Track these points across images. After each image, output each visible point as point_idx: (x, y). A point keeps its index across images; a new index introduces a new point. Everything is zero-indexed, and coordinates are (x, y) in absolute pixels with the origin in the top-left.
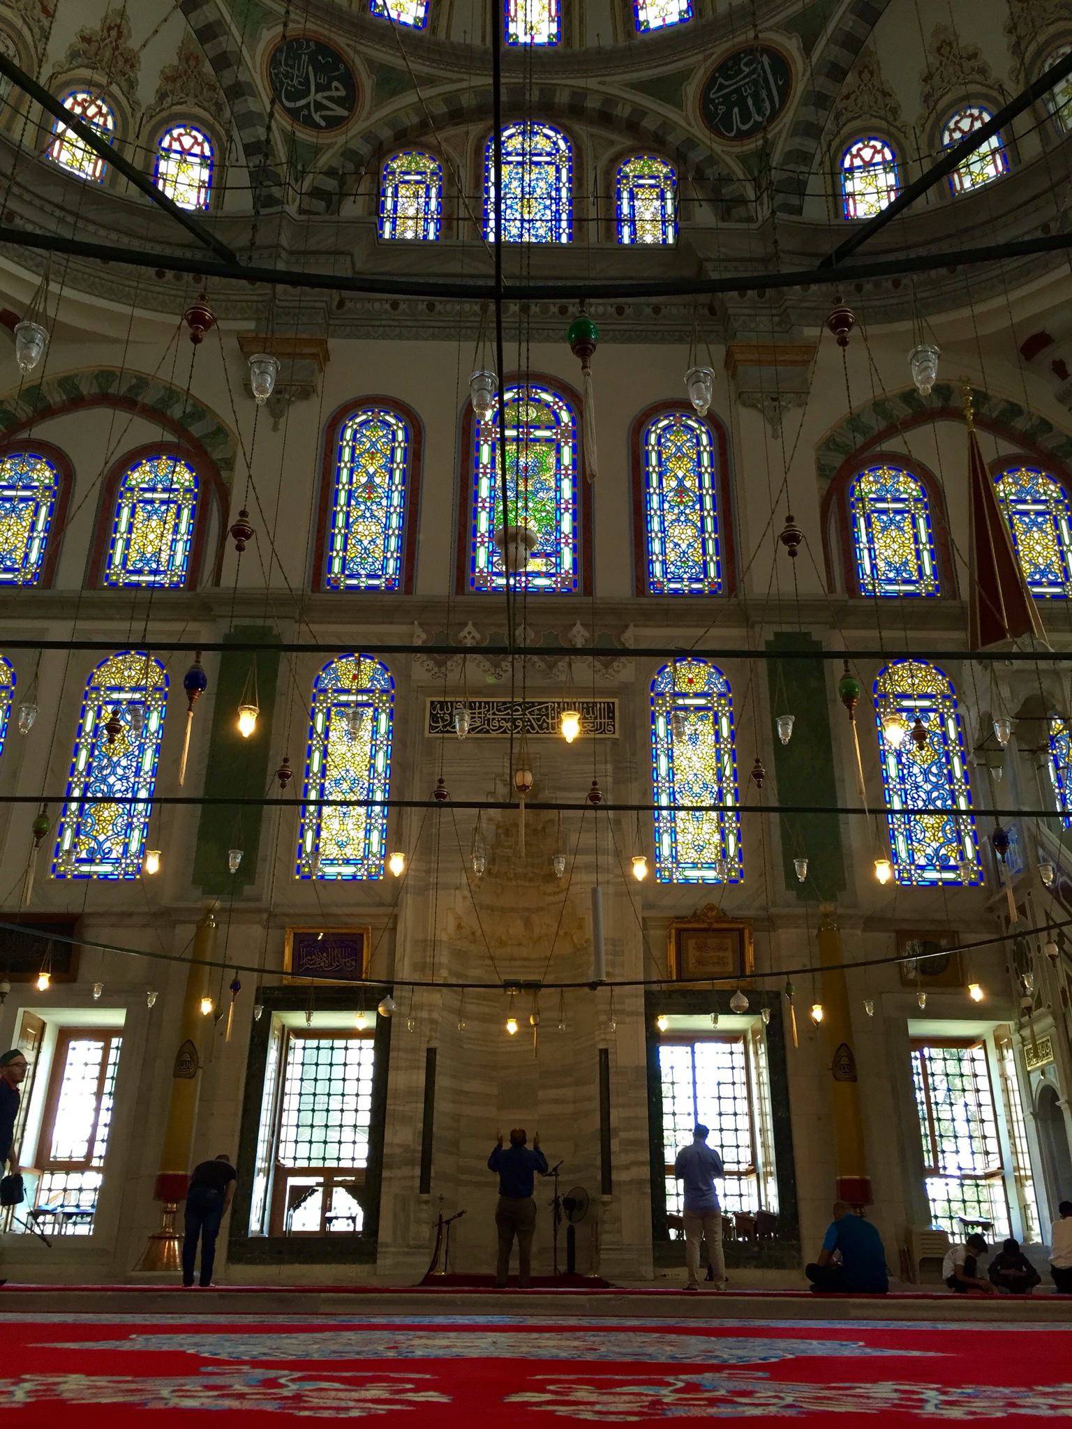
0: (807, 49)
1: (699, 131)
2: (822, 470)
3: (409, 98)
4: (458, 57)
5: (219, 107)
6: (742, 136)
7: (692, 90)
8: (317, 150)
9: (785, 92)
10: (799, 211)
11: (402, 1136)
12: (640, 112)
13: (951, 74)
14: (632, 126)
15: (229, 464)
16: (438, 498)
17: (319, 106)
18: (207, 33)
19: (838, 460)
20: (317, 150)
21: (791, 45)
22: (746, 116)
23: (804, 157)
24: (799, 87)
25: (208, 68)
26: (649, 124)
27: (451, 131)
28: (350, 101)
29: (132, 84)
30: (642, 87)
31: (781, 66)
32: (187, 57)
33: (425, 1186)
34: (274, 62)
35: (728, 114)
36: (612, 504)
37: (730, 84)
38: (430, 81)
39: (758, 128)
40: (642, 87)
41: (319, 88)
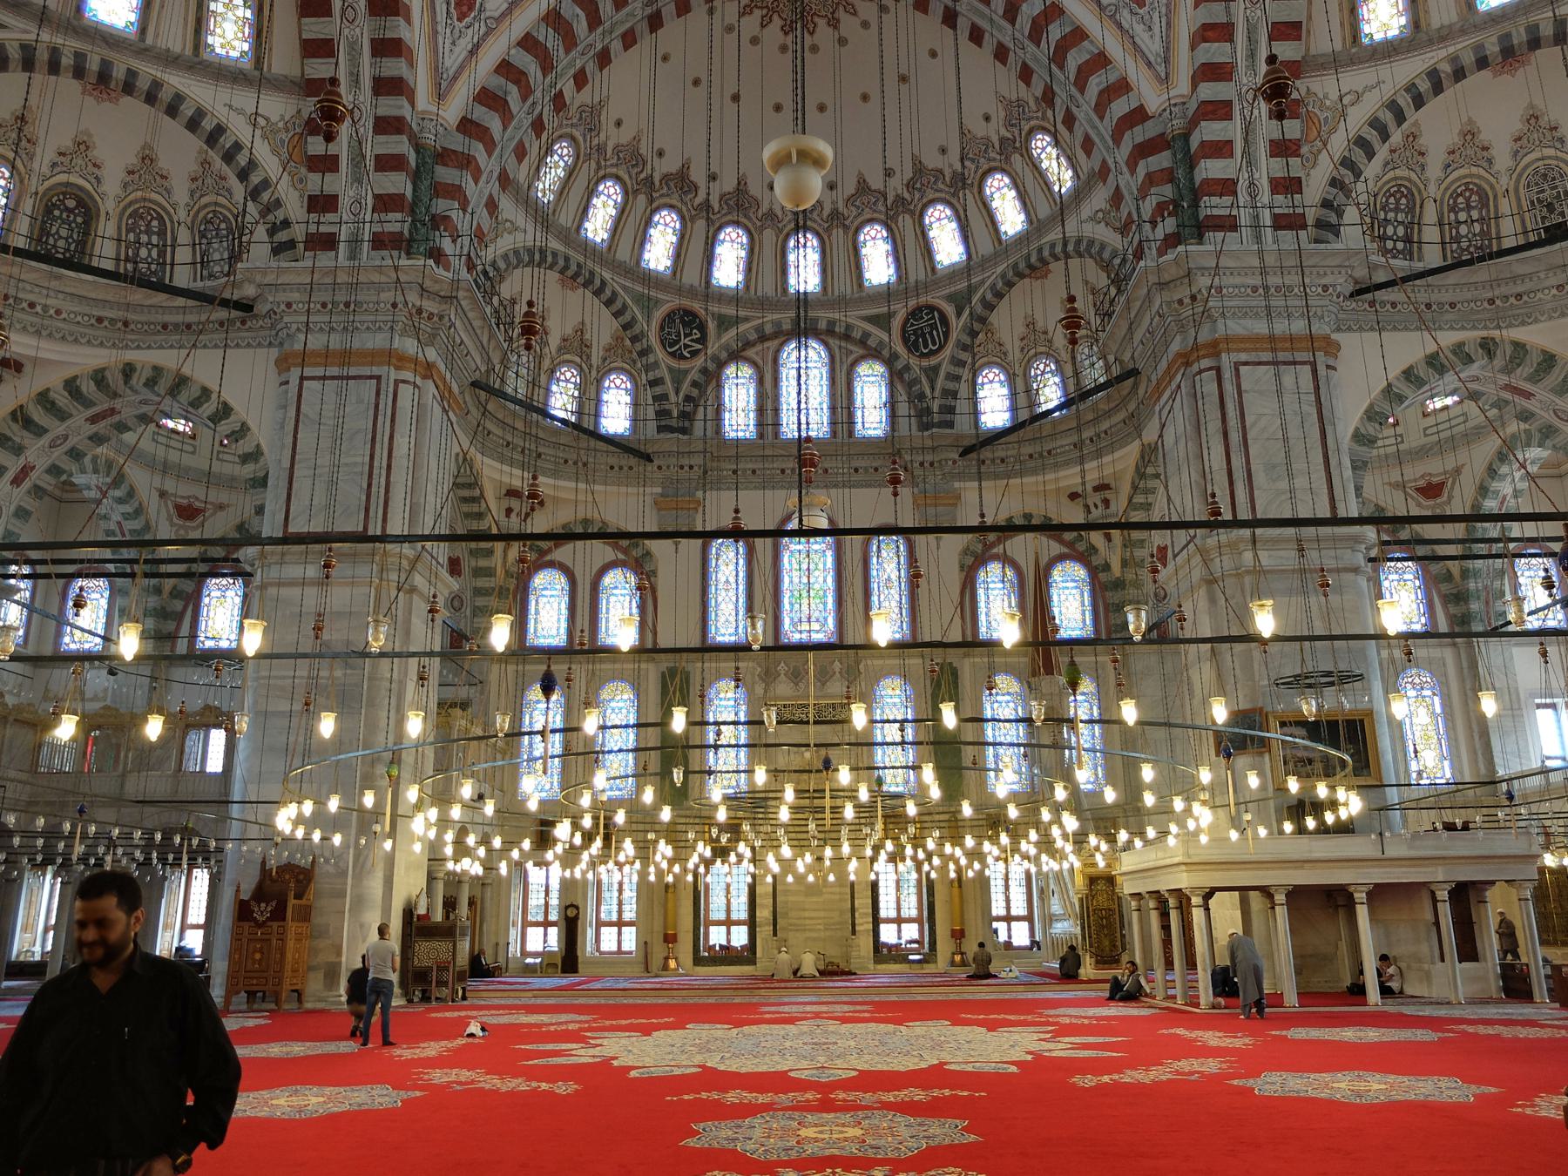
0: (959, 314)
1: (900, 348)
2: (962, 567)
3: (732, 332)
4: (763, 304)
5: (634, 362)
6: (923, 355)
7: (896, 324)
8: (687, 372)
9: (947, 335)
10: (951, 425)
11: (764, 914)
12: (866, 335)
13: (1035, 344)
14: (862, 342)
15: (654, 573)
16: (764, 593)
17: (686, 346)
18: (626, 327)
19: (970, 560)
20: (687, 372)
21: (950, 310)
22: (926, 346)
23: (958, 378)
24: (954, 336)
25: (628, 343)
26: (872, 342)
27: (759, 347)
28: (703, 340)
29: (589, 357)
30: (870, 319)
31: (944, 320)
32: (618, 339)
33: (775, 934)
34: (662, 328)
35: (916, 341)
36: (853, 592)
37: (918, 324)
38: (747, 319)
39: (933, 353)
40: (870, 319)
41: (686, 336)
